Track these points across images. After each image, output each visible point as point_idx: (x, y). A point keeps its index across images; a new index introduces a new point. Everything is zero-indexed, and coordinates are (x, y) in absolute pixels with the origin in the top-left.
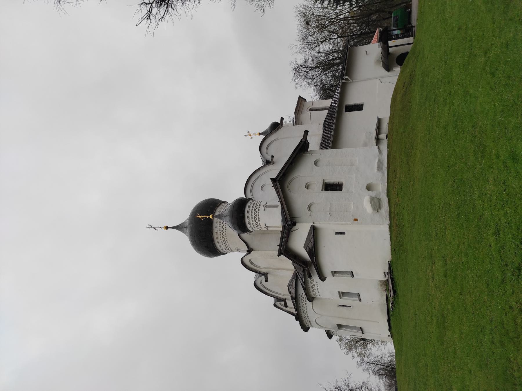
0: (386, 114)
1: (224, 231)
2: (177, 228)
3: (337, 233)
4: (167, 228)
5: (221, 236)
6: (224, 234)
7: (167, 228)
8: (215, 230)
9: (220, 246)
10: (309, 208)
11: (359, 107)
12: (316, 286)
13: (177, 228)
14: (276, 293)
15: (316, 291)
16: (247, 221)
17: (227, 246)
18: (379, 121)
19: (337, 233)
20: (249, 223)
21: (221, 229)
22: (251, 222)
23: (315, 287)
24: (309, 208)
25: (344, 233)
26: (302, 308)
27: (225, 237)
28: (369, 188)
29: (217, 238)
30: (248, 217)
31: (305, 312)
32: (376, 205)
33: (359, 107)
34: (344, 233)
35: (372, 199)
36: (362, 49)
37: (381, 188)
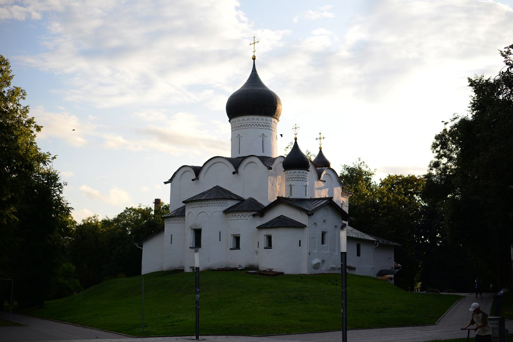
0: (357, 272)
1: (259, 127)
2: (254, 70)
3: (300, 241)
4: (254, 59)
5: (255, 124)
6: (256, 126)
7: (254, 59)
8: (260, 118)
9: (244, 120)
10: (315, 224)
11: (358, 254)
12: (244, 218)
13: (254, 70)
14: (206, 173)
15: (239, 218)
16: (297, 171)
17: (244, 127)
18: (354, 269)
19: (300, 241)
20: (295, 172)
21: (261, 124)
22: (295, 174)
23: (243, 218)
24: (315, 224)
25: (300, 246)
26: (216, 202)
27: (253, 127)
28: (323, 261)
29: (253, 119)
30: (299, 172)
31: (212, 205)
32: (316, 266)
33: (358, 254)
34: (300, 246)
35: (319, 264)
36: (391, 255)
37: (323, 269)
